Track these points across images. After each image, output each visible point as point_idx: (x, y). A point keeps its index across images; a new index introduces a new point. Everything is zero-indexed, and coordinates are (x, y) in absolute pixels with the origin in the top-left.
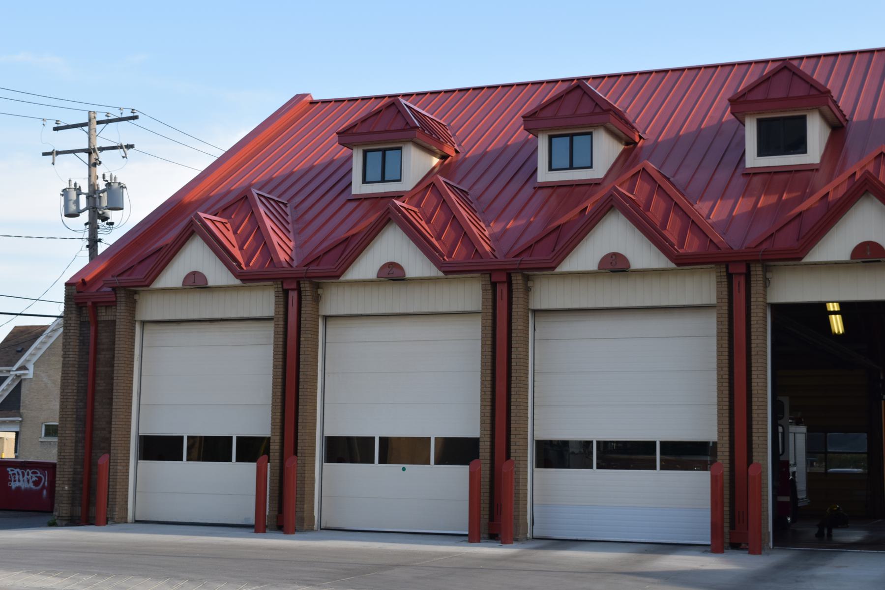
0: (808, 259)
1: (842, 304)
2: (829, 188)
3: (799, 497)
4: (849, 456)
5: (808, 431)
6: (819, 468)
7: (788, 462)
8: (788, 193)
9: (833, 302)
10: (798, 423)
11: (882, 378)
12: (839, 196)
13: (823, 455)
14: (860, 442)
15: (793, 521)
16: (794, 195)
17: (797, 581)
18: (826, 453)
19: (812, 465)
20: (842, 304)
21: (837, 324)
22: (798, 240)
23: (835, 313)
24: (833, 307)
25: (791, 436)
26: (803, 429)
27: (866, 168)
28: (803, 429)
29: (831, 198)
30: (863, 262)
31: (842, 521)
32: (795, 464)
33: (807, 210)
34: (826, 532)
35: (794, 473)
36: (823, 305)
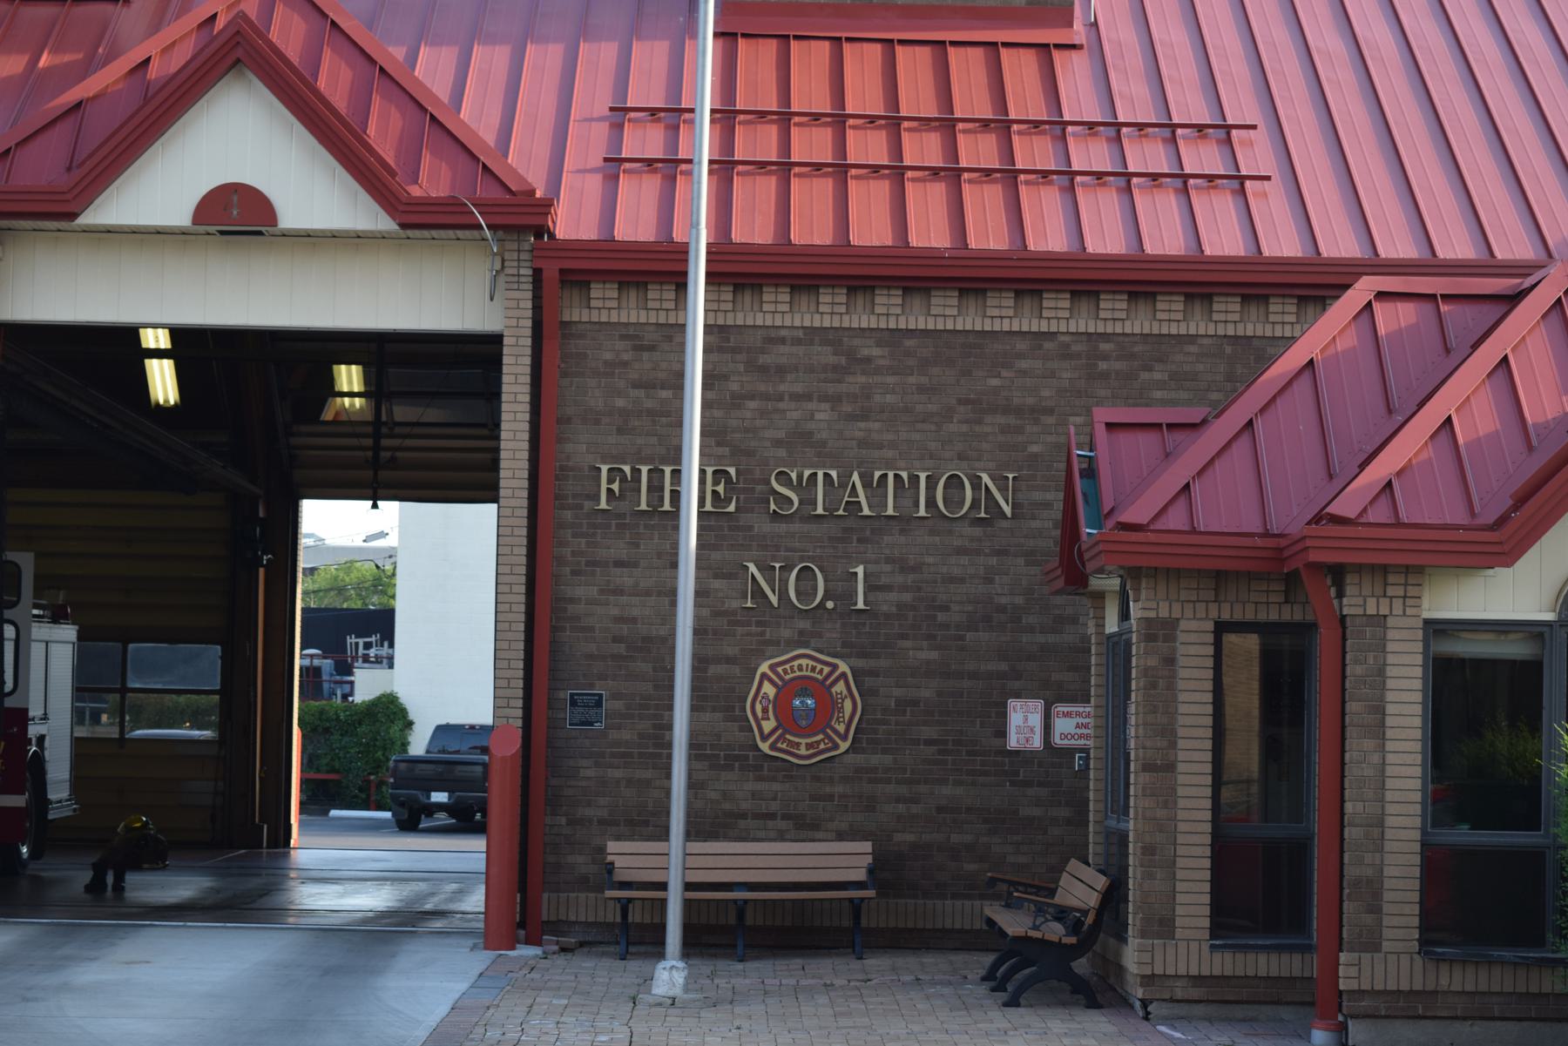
0: (89, 218)
1: (177, 333)
2: (151, 47)
3: (52, 796)
4: (182, 699)
5: (80, 638)
6: (107, 727)
7: (26, 710)
8: (55, 51)
9: (155, 326)
10: (57, 616)
11: (261, 514)
12: (173, 69)
13: (117, 696)
14: (203, 665)
15: (34, 855)
16: (67, 58)
17: (26, 1000)
18: (124, 690)
19: (95, 719)
20: (177, 333)
21: (163, 382)
22: (69, 169)
23: (158, 354)
24: (156, 339)
25: (37, 651)
26: (69, 632)
27: (242, 6)
28: (69, 632)
29: (154, 72)
30: (222, 233)
31: (149, 854)
32: (45, 717)
33: (95, 97)
34: (110, 879)
35: (41, 739)
36: (128, 335)
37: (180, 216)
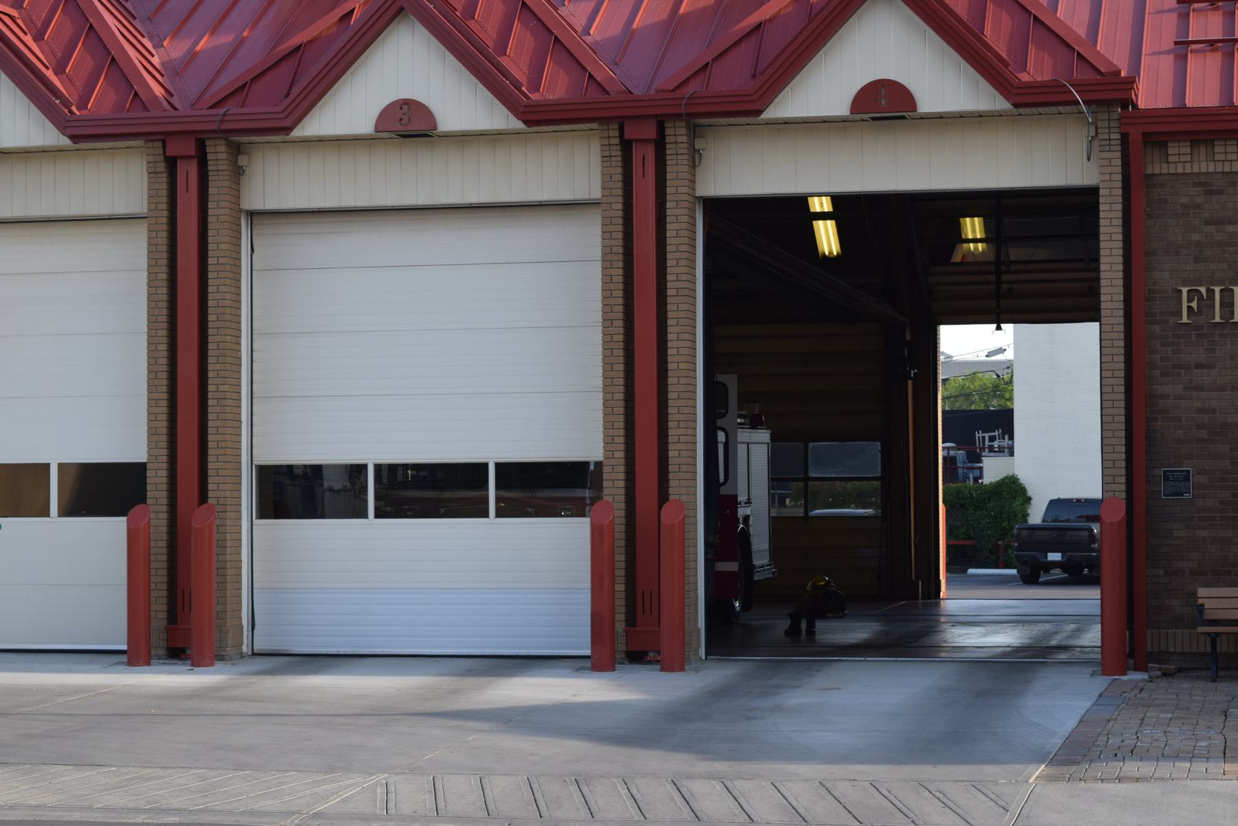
0: (772, 113)
1: (836, 199)
3: (756, 562)
4: (849, 485)
5: (772, 439)
6: (793, 509)
7: (736, 496)
9: (820, 195)
10: (755, 424)
14: (868, 458)
17: (749, 718)
18: (806, 479)
19: (782, 503)
20: (836, 199)
21: (827, 238)
22: (754, 76)
23: (823, 216)
24: (820, 204)
25: (742, 449)
26: (764, 435)
28: (764, 435)
30: (874, 119)
31: (834, 605)
32: (749, 502)
33: (771, 19)
34: (804, 626)
35: (746, 518)
36: (800, 202)
37: (841, 107)
